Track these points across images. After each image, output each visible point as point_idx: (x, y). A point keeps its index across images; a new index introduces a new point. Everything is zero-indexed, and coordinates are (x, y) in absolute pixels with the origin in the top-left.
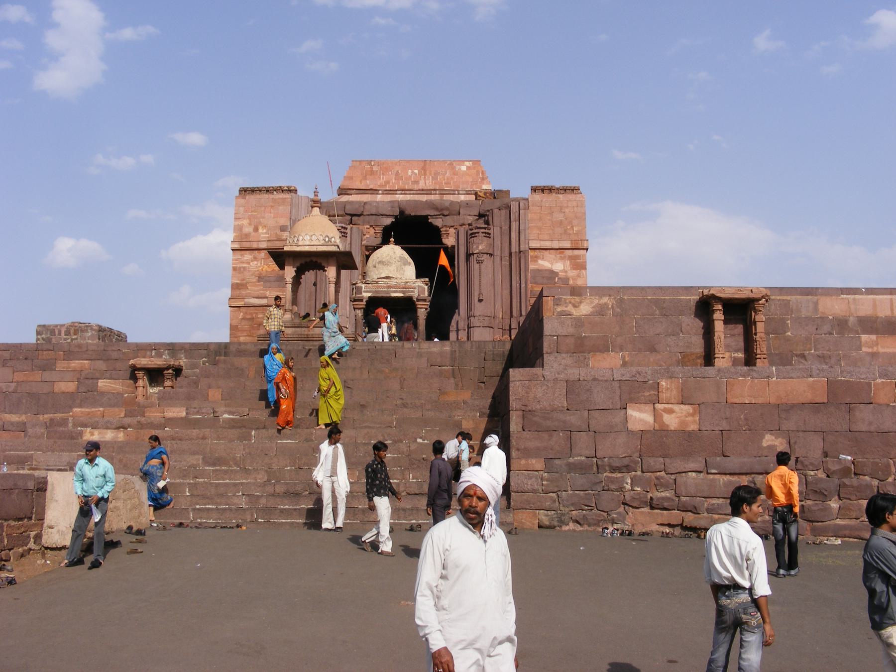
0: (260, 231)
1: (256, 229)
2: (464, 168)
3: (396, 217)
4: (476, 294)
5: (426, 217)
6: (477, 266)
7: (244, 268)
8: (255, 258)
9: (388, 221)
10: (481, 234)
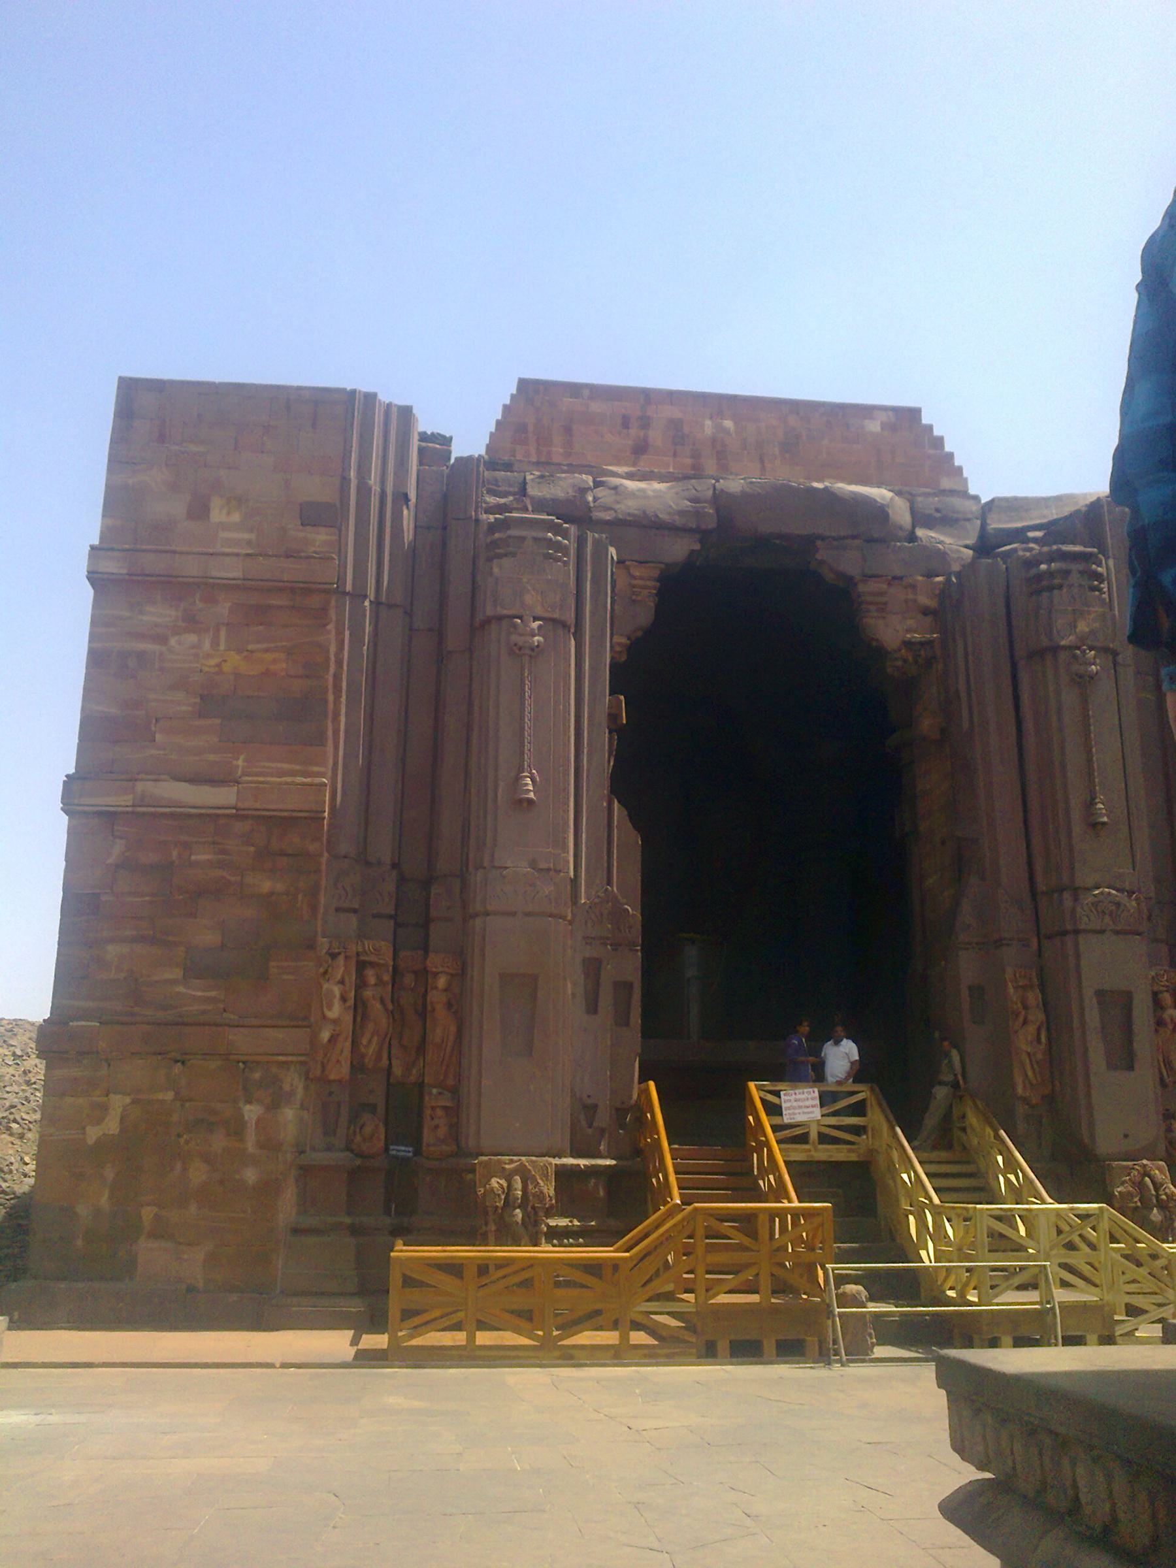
0: (218, 515)
1: (199, 510)
2: (873, 426)
3: (704, 535)
4: (1076, 802)
5: (810, 542)
6: (1069, 697)
7: (141, 656)
8: (191, 623)
9: (678, 550)
10: (1075, 578)
